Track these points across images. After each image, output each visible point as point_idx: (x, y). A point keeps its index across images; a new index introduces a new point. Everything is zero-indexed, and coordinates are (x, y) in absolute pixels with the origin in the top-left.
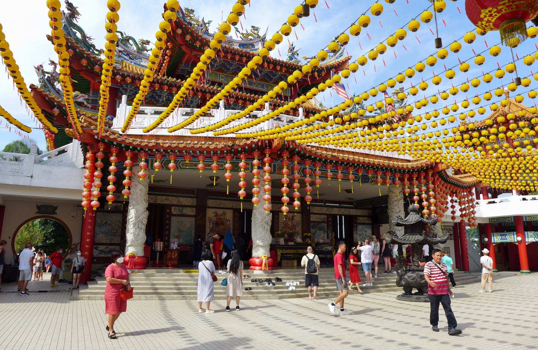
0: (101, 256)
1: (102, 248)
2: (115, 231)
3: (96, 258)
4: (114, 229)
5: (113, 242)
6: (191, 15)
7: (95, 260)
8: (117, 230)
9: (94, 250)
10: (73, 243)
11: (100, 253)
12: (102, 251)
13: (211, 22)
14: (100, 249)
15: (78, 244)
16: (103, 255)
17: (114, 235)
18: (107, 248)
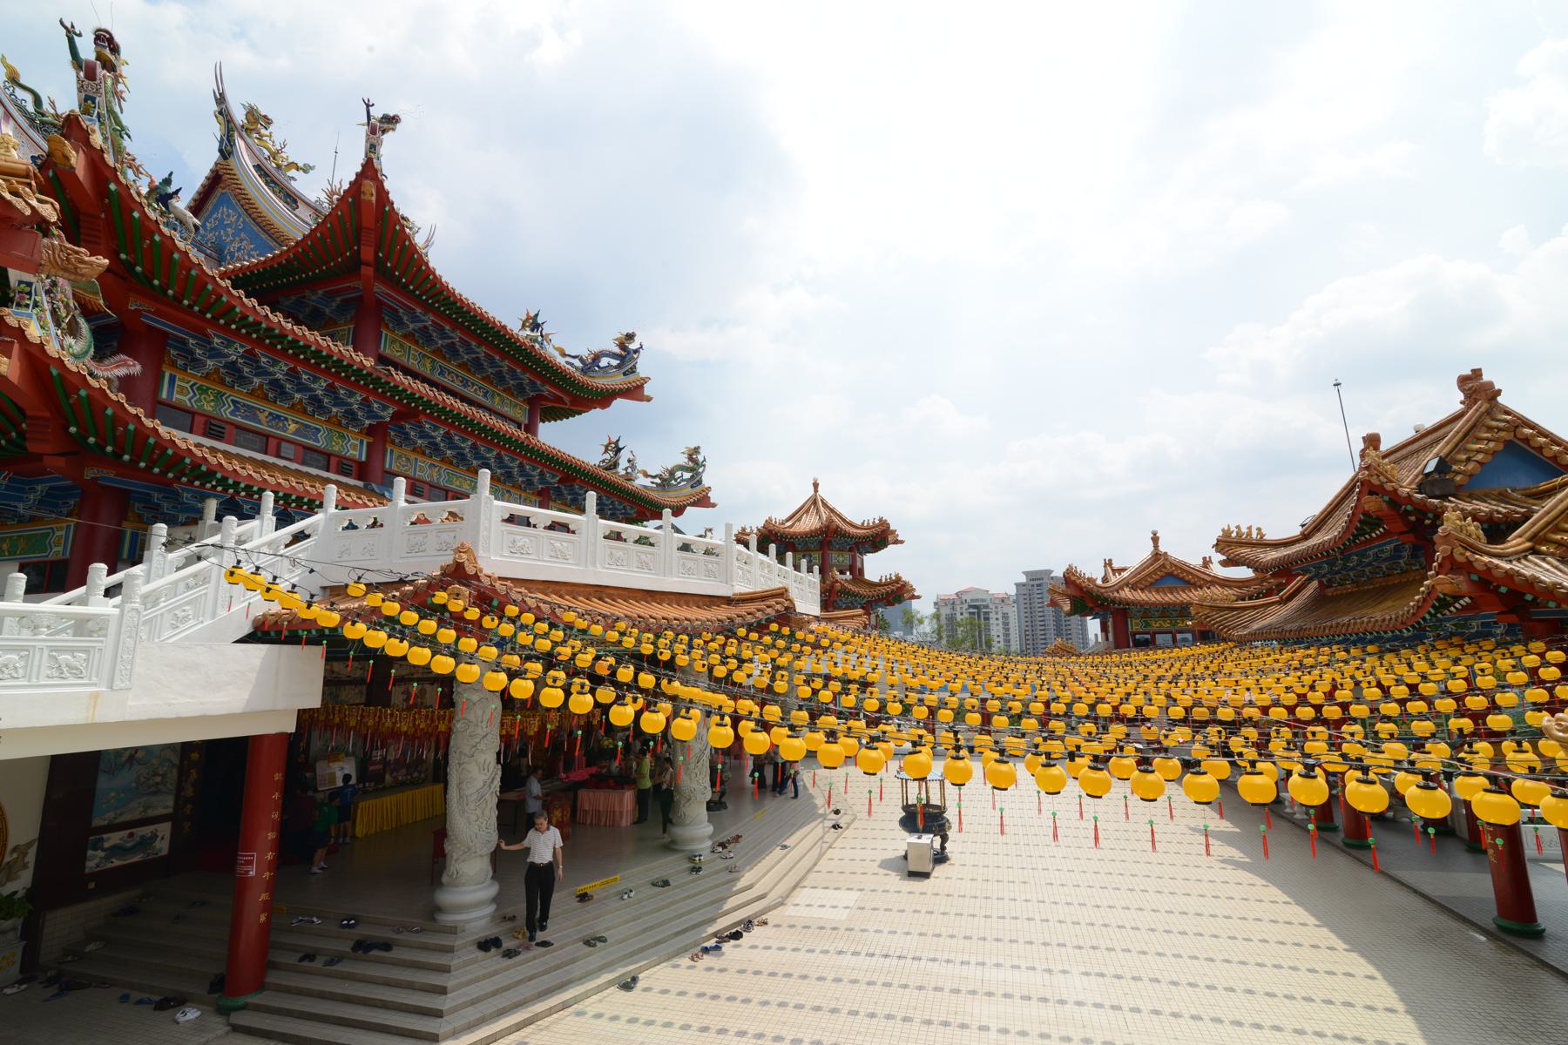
0: (109, 866)
1: (114, 838)
2: (158, 779)
3: (94, 876)
4: (155, 774)
5: (151, 813)
6: (263, 131)
7: (92, 885)
8: (164, 776)
9: (90, 852)
10: (10, 845)
11: (107, 858)
12: (116, 850)
13: (312, 168)
14: (106, 845)
15: (30, 844)
16: (117, 863)
17: (154, 793)
18: (131, 835)
